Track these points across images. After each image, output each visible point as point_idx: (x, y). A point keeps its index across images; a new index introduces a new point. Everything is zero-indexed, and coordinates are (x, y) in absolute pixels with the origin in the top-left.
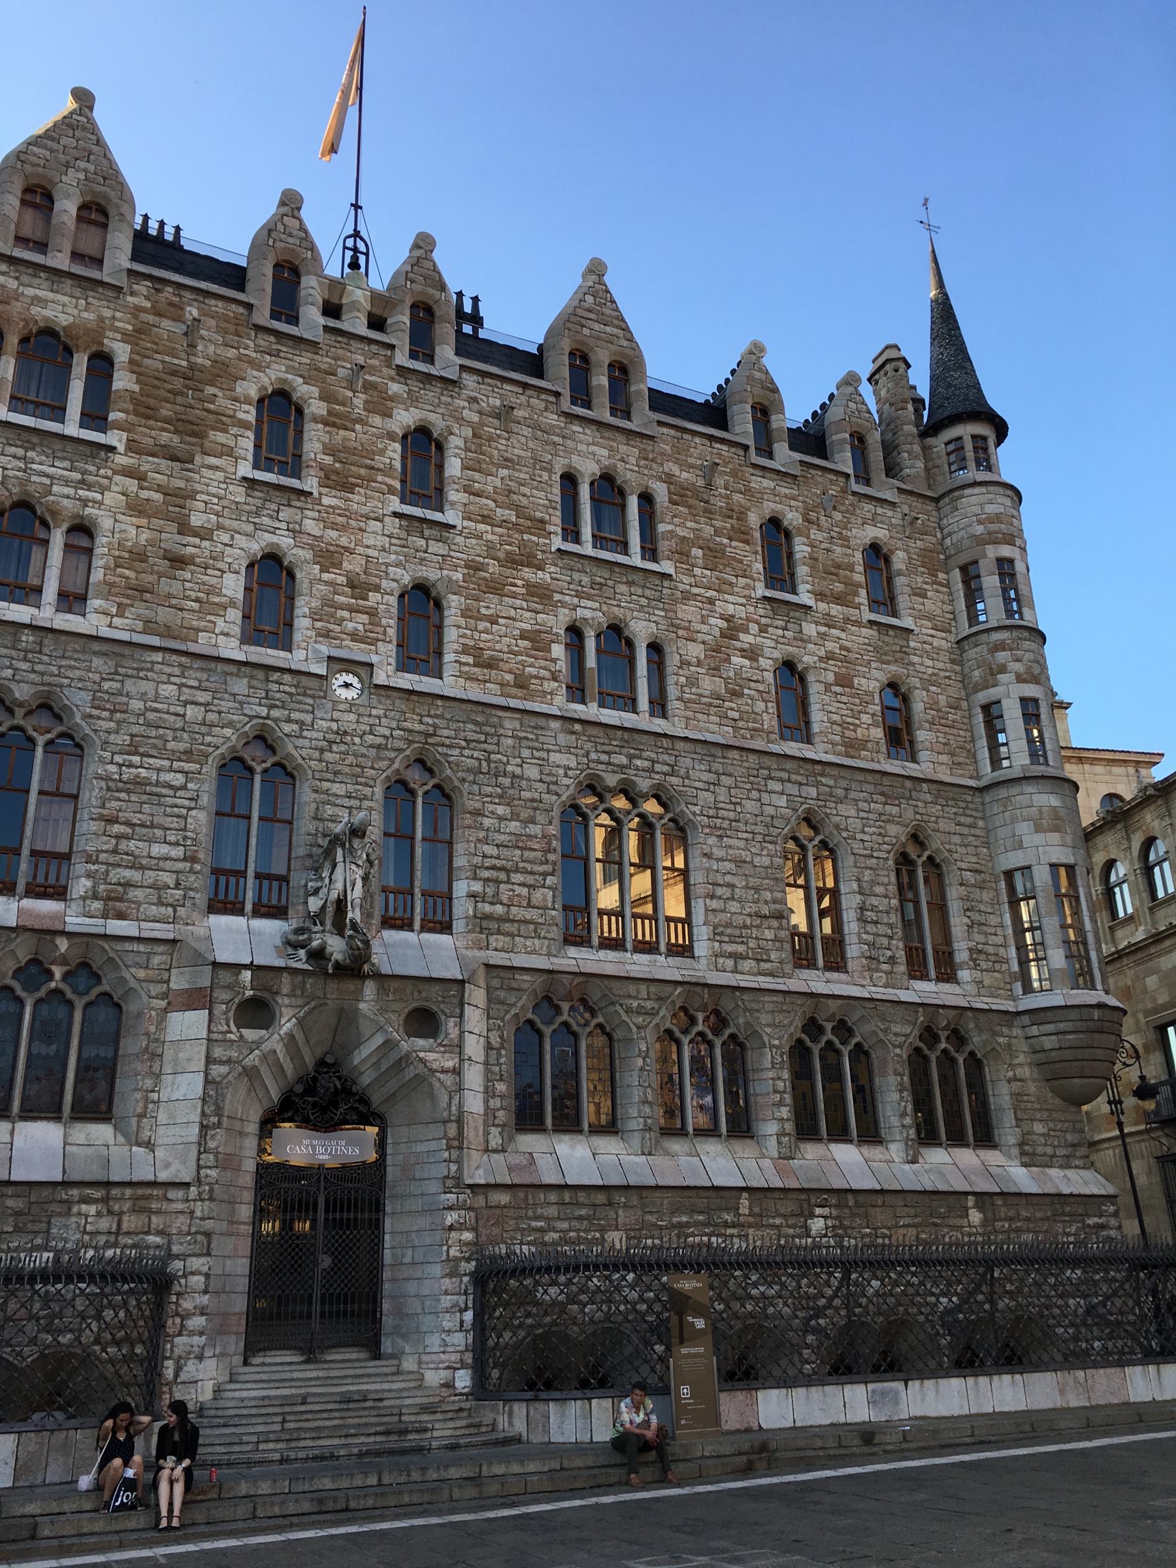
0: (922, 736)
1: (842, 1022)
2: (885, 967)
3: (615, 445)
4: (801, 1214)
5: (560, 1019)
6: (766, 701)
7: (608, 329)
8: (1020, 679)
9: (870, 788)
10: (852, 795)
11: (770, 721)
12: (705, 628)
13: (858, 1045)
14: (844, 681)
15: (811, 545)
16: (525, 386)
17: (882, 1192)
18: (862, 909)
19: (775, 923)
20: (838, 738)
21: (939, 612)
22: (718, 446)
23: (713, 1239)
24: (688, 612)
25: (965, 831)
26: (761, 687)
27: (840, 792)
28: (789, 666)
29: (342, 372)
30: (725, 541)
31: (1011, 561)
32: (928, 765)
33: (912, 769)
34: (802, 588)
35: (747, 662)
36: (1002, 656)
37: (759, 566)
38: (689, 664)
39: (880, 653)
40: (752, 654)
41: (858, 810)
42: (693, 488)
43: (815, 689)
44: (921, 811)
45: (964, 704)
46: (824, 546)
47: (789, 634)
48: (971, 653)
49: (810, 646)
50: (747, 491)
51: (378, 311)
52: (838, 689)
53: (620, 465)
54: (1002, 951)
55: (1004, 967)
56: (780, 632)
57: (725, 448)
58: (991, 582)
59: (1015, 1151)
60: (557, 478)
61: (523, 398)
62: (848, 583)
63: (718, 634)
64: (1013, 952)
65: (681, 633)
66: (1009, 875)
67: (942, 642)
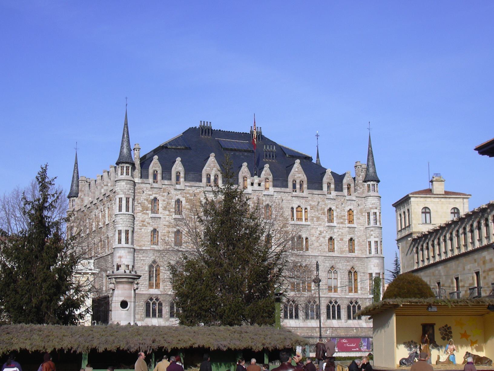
0: (356, 248)
1: (336, 301)
2: (345, 292)
3: (300, 200)
4: (326, 331)
5: (290, 303)
6: (326, 246)
7: (300, 175)
8: (375, 237)
9: (344, 260)
10: (341, 262)
11: (327, 250)
12: (316, 234)
13: (339, 305)
14: (341, 240)
15: (337, 213)
16: (285, 192)
17: (339, 327)
18: (341, 282)
19: (325, 286)
20: (339, 251)
21: (362, 222)
22: (320, 195)
23: (312, 334)
24: (313, 231)
25: (362, 266)
26: (326, 243)
27: (339, 261)
28: (331, 239)
29: (255, 198)
30: (320, 215)
31: (376, 213)
32: (357, 253)
33: (353, 255)
34: (335, 222)
35: (323, 239)
36: (372, 232)
37: (326, 220)
38: (313, 241)
39: (349, 233)
40: (324, 237)
41: (342, 264)
42: (314, 206)
43: (335, 242)
44: (354, 263)
45: (366, 241)
46: (340, 212)
47: (331, 232)
48: (367, 231)
49: (335, 234)
50: (325, 204)
51: (260, 183)
52: (340, 241)
53: (301, 204)
54: (367, 287)
55: (367, 290)
56: (330, 232)
57: (321, 195)
58: (372, 217)
59: (364, 321)
60: (290, 209)
61: (284, 195)
62: (344, 220)
63: (318, 234)
64: (369, 287)
65: (311, 235)
66: (369, 273)
67: (362, 228)
